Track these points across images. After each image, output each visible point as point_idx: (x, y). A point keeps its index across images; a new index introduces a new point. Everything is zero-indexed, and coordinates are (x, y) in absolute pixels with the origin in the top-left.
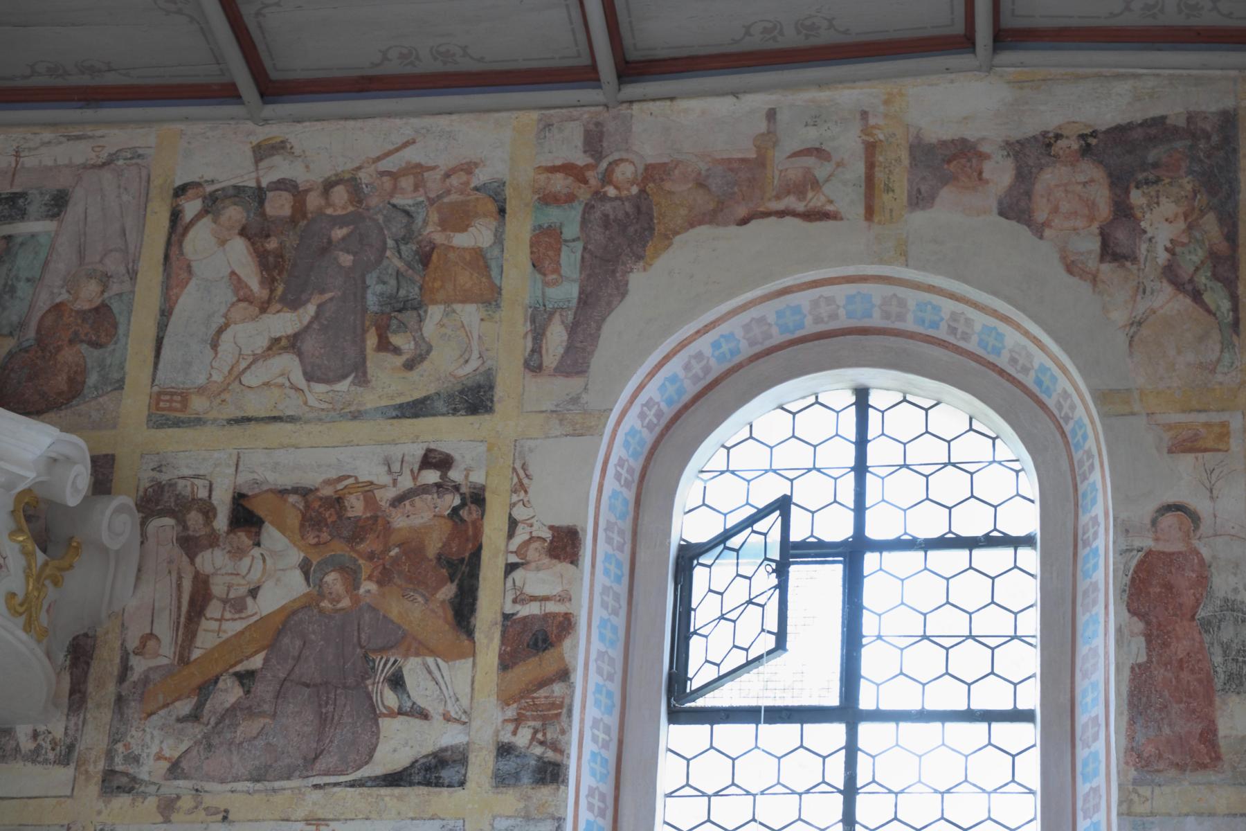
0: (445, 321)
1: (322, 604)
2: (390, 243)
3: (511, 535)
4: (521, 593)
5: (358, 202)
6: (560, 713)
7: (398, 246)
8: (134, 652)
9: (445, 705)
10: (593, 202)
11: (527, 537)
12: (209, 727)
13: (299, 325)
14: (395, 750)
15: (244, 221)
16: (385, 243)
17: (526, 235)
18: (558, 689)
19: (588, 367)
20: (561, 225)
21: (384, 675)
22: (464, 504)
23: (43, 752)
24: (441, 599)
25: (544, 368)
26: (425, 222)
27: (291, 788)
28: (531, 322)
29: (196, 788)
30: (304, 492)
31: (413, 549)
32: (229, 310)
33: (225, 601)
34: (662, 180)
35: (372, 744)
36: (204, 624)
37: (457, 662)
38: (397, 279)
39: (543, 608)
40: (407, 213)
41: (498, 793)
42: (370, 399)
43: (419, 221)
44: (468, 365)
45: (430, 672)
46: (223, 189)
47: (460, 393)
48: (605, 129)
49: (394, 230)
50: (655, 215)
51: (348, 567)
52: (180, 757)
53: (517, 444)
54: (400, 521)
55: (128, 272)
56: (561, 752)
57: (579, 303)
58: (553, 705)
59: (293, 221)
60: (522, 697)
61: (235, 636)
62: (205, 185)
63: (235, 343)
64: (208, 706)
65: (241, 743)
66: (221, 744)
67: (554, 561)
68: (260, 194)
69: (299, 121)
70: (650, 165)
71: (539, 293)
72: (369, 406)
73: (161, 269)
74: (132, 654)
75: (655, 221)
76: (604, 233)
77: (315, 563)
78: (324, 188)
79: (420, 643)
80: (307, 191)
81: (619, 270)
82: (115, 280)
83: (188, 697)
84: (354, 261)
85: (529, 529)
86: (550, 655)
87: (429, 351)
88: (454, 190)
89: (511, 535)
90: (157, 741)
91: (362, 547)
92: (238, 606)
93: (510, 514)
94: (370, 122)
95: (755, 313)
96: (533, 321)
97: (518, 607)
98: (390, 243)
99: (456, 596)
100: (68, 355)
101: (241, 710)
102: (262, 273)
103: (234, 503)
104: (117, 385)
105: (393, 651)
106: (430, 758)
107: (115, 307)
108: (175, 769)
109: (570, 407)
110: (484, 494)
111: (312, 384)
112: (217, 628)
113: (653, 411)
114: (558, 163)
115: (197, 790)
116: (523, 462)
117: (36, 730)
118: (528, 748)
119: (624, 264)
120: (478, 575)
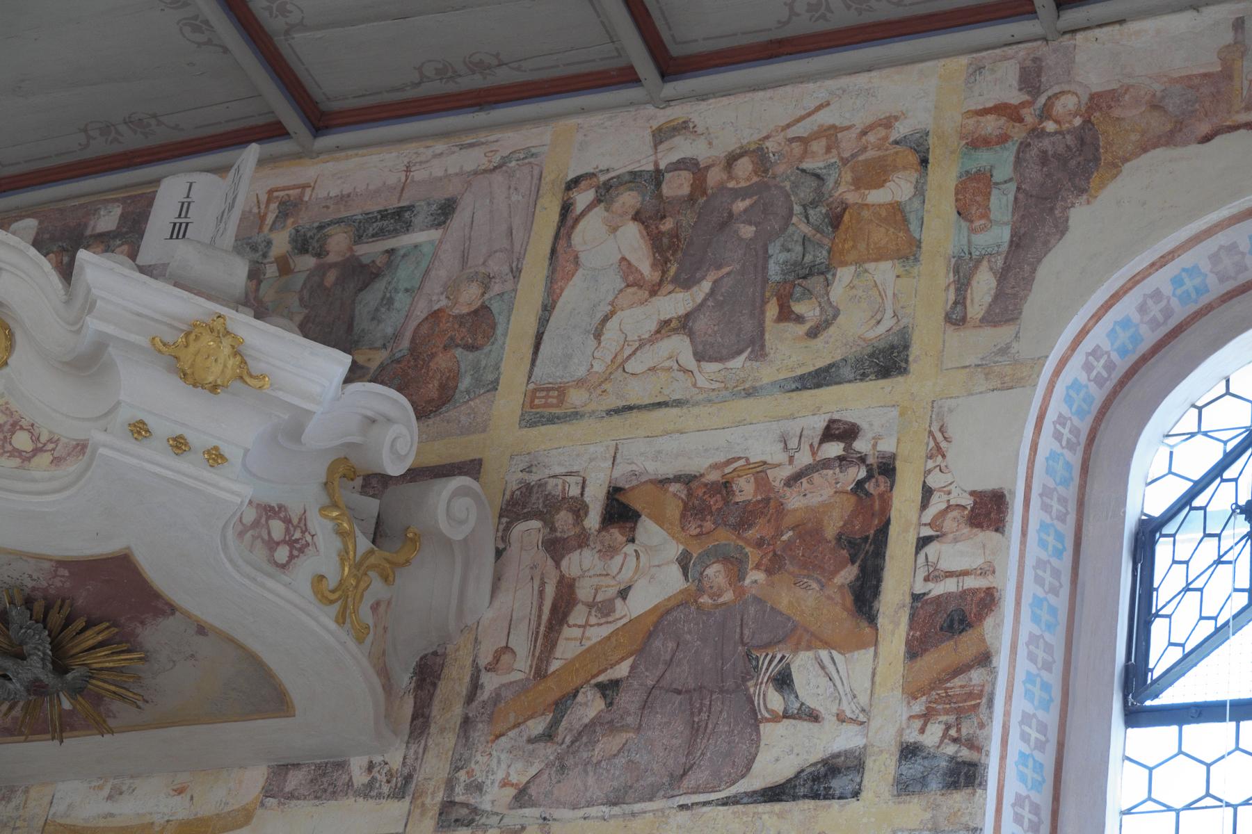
0: (856, 282)
1: (701, 600)
2: (797, 209)
3: (924, 505)
4: (935, 569)
5: (763, 172)
6: (980, 703)
7: (806, 210)
8: (486, 668)
9: (839, 703)
10: (1029, 140)
11: (944, 506)
12: (564, 746)
13: (691, 305)
14: (777, 760)
15: (638, 205)
16: (791, 209)
17: (951, 182)
18: (976, 676)
19: (1020, 313)
20: (992, 167)
21: (768, 674)
22: (870, 476)
23: (377, 785)
24: (839, 583)
25: (968, 319)
26: (837, 183)
27: (653, 811)
28: (954, 272)
29: (543, 816)
30: (687, 480)
31: (809, 531)
32: (616, 297)
33: (590, 606)
34: (1110, 107)
35: (751, 753)
36: (567, 632)
37: (856, 653)
38: (804, 244)
39: (961, 584)
40: (818, 176)
41: (900, 803)
42: (767, 373)
43: (830, 183)
44: (879, 326)
45: (823, 668)
46: (618, 177)
47: (869, 357)
48: (1044, 64)
49: (802, 195)
50: (1101, 144)
51: (733, 557)
52: (528, 782)
53: (935, 405)
54: (795, 501)
55: (512, 271)
56: (979, 749)
57: (1010, 246)
58: (970, 695)
59: (691, 199)
60: (933, 689)
61: (600, 643)
62: (600, 175)
63: (621, 330)
64: (563, 723)
65: (599, 762)
66: (576, 765)
67: (975, 530)
68: (657, 177)
69: (703, 97)
70: (1096, 93)
71: (965, 241)
72: (765, 381)
73: (547, 263)
74: (483, 671)
75: (1101, 151)
76: (1042, 170)
77: (695, 555)
78: (728, 163)
79: (813, 634)
80: (708, 168)
81: (1058, 207)
82: (497, 281)
83: (543, 714)
84: (756, 231)
85: (945, 497)
86: (968, 639)
87: (835, 317)
88: (869, 148)
89: (924, 505)
90: (504, 766)
91: (752, 534)
92: (605, 609)
93: (924, 482)
94: (781, 91)
95: (1222, 239)
96: (957, 271)
97: (931, 585)
98: (797, 209)
99: (857, 579)
100: (442, 362)
101: (601, 724)
102: (654, 256)
103: (608, 498)
104: (490, 386)
105: (780, 646)
106: (819, 766)
107: (495, 307)
108: (522, 797)
109: (998, 358)
110: (894, 463)
111: (703, 364)
112: (580, 636)
113: (1102, 361)
114: (990, 104)
115: (545, 819)
116: (941, 424)
117: (371, 762)
118: (938, 747)
119: (1064, 199)
120: (885, 553)
